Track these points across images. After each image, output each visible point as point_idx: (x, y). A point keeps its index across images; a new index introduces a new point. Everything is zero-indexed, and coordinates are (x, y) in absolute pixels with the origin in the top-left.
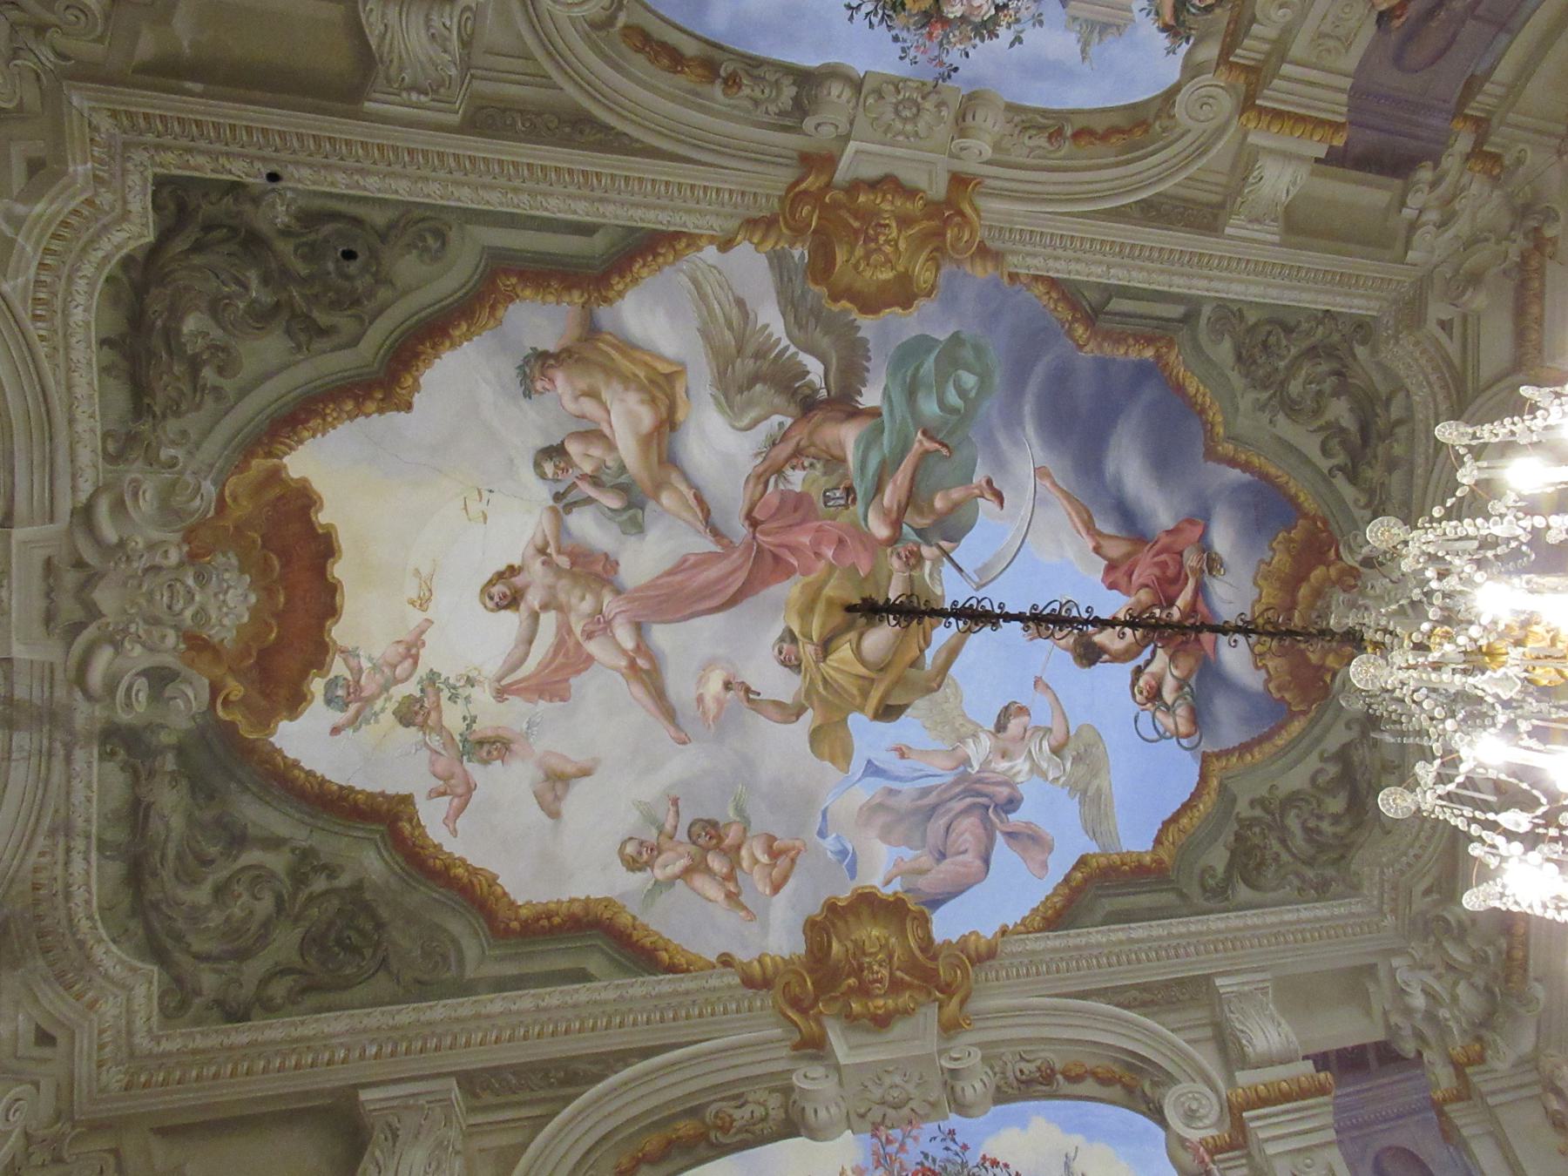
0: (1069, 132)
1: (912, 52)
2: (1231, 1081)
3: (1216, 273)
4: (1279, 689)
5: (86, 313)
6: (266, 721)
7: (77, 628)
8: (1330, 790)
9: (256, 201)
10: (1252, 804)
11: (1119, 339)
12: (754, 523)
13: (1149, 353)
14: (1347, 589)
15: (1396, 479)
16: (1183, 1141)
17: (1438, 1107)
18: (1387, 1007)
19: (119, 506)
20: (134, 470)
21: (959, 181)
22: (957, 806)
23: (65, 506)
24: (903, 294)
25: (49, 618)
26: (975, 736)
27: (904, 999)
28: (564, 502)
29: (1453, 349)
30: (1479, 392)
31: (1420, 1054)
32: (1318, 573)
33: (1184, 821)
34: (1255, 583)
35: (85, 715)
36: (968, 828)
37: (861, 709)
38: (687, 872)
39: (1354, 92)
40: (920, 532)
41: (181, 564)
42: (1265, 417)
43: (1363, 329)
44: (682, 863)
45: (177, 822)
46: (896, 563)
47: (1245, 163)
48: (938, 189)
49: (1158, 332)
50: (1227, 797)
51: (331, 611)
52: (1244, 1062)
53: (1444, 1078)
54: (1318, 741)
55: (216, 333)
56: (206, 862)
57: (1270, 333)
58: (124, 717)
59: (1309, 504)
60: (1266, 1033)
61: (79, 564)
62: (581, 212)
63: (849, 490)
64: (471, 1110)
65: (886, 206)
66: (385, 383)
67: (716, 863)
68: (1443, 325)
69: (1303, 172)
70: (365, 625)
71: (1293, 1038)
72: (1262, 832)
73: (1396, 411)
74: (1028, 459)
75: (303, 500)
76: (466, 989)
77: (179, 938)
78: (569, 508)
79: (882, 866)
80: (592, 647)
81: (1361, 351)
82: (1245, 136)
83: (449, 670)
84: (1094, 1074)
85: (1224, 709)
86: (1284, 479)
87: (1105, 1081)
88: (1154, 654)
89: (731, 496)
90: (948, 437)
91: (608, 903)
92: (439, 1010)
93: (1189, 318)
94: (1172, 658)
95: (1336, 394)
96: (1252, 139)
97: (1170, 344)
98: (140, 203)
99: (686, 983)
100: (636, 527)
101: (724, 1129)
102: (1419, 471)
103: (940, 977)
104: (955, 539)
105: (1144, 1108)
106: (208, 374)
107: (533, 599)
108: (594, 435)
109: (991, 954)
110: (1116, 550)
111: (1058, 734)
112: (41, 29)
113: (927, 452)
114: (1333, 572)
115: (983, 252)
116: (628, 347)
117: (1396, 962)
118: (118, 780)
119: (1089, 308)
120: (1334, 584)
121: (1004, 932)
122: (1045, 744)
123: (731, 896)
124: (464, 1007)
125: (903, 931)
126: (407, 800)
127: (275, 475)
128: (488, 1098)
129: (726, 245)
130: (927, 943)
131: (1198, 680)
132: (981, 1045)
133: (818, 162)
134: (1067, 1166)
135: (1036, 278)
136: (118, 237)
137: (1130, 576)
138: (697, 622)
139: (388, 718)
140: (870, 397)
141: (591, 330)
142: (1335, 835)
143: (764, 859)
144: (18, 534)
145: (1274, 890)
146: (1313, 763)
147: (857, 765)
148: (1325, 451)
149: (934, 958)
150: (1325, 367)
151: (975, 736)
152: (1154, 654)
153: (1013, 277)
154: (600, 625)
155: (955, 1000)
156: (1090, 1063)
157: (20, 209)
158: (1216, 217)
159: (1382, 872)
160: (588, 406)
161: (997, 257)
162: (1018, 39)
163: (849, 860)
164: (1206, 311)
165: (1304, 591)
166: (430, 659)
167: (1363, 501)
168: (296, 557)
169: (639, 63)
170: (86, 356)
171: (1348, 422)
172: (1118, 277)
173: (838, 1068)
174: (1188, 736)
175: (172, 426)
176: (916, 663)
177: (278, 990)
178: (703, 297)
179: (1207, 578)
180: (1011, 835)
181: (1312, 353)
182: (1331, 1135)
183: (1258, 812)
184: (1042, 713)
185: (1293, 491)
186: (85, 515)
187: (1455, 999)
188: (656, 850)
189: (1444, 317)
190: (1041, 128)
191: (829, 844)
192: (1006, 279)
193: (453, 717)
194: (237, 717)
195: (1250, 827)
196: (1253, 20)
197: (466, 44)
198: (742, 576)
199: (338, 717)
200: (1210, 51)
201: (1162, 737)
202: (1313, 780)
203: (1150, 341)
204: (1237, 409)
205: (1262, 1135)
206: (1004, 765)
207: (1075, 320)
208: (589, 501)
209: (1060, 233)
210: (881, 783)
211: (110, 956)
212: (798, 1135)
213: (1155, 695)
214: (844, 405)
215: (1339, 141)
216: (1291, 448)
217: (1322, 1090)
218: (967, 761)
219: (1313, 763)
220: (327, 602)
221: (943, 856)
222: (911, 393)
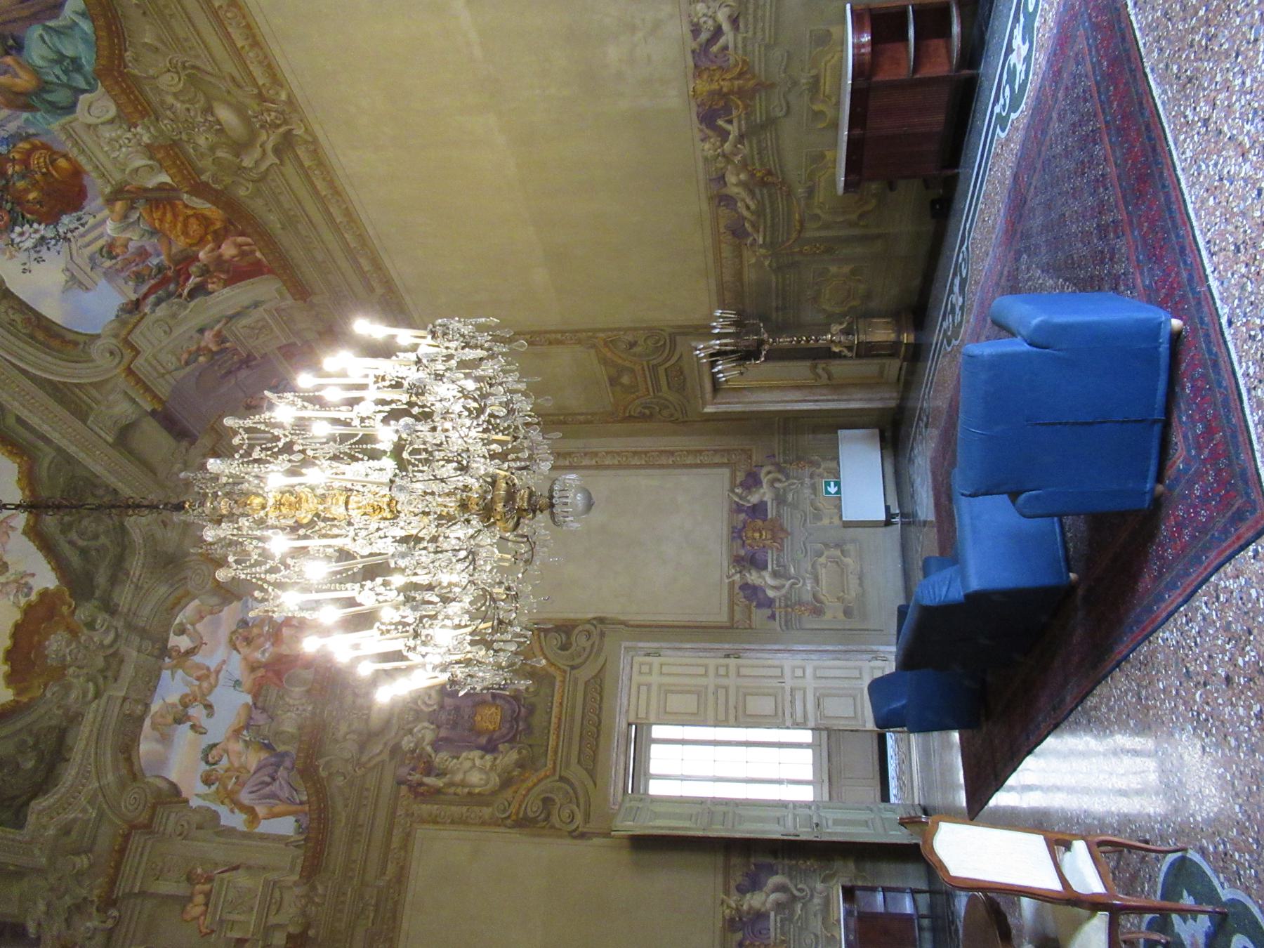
5: (69, 774)
7: (115, 654)
19: (85, 694)
23: (105, 698)
25: (122, 661)
41: (70, 666)
45: (102, 570)
51: (17, 627)
56: (97, 550)
58: (107, 616)
61: (105, 678)
64: (91, 409)
75: (11, 679)
76: (59, 450)
92: (72, 450)
98: (32, 819)
106: (31, 742)
112: (52, 889)
118: (115, 596)
124: (63, 443)
126: (25, 533)
127: (19, 693)
128: (84, 407)
139: (11, 571)
144: (122, 694)
170: (76, 756)
175: (54, 722)
177: (100, 492)
186: (98, 695)
194: (68, 598)
199: (31, 581)
212: (7, 290)
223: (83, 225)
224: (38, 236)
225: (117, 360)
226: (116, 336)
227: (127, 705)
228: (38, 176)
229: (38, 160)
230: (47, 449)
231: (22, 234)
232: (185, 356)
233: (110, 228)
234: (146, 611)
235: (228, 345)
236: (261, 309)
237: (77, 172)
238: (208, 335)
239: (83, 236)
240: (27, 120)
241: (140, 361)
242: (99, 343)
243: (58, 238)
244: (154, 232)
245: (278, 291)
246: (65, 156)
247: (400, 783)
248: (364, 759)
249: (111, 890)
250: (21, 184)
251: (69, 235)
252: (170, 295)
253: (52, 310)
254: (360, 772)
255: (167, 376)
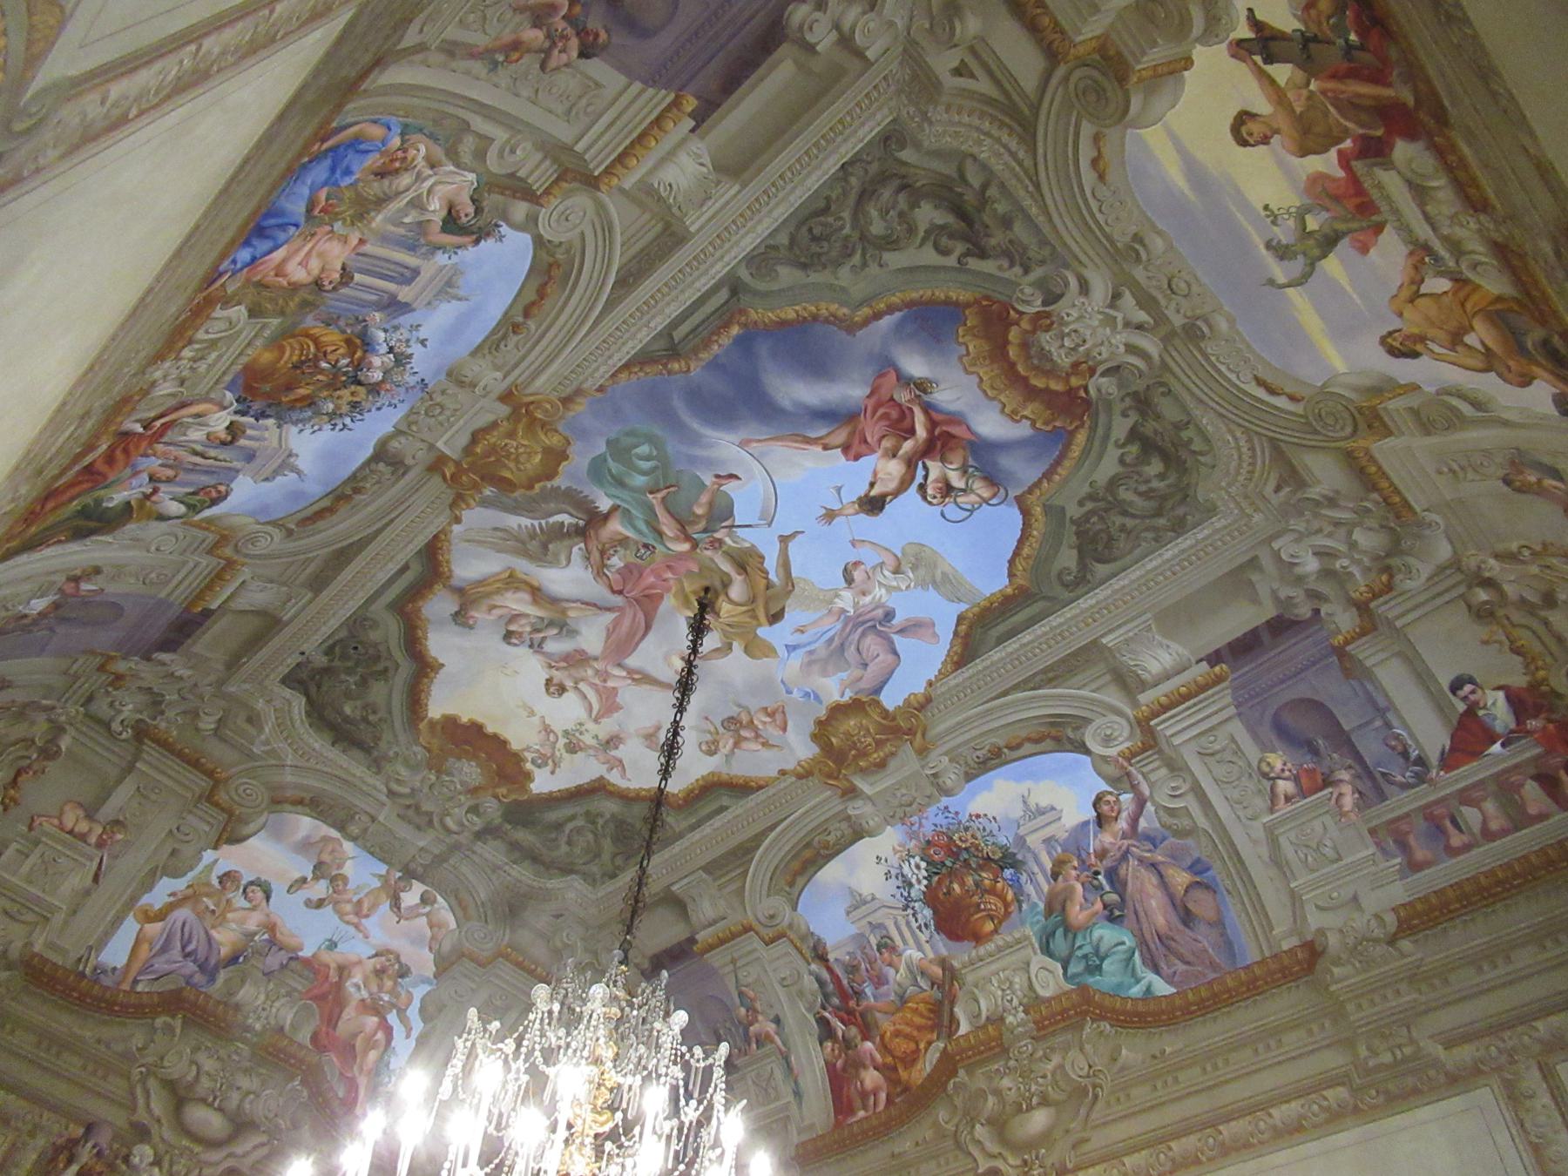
0: (520, 319)
1: (395, 401)
2: (1135, 704)
3: (718, 254)
4: (1046, 423)
5: (318, 742)
6: (524, 788)
7: (430, 823)
8: (1144, 458)
9: (309, 662)
10: (1081, 503)
11: (706, 344)
12: (620, 592)
13: (735, 330)
14: (1048, 329)
15: (1019, 229)
16: (1104, 758)
17: (1340, 652)
18: (1275, 586)
19: (398, 782)
20: (388, 768)
21: (506, 397)
22: (856, 636)
23: (384, 798)
24: (556, 457)
25: (419, 828)
26: (837, 596)
27: (888, 748)
28: (537, 647)
29: (984, 86)
30: (1036, 108)
31: (1317, 612)
32: (1014, 335)
33: (1026, 551)
34: (967, 372)
35: (464, 838)
36: (871, 644)
37: (760, 625)
38: (736, 745)
39: (651, 81)
40: (705, 531)
42: (873, 269)
43: (891, 139)
44: (731, 741)
46: (708, 553)
47: (647, 195)
48: (504, 410)
49: (725, 317)
50: (1055, 513)
51: (505, 743)
52: (1144, 686)
53: (1344, 620)
54: (1106, 437)
55: (359, 703)
57: (810, 230)
59: (964, 296)
60: (1158, 659)
61: (409, 807)
62: (393, 567)
63: (646, 546)
64: (715, 880)
65: (493, 440)
66: (424, 667)
67: (744, 733)
68: (958, 72)
69: (697, 145)
70: (520, 736)
71: (1181, 650)
72: (1101, 518)
73: (975, 180)
74: (726, 446)
75: (450, 723)
76: (681, 836)
77: (572, 863)
78: (540, 645)
79: (834, 688)
80: (610, 684)
81: (906, 155)
82: (622, 191)
83: (570, 726)
84: (1029, 739)
85: (1006, 462)
86: (929, 293)
87: (1037, 741)
88: (925, 468)
89: (596, 590)
90: (666, 481)
91: (713, 773)
93: (734, 292)
94: (943, 460)
95: (914, 205)
96: (627, 186)
97: (742, 312)
98: (287, 693)
99: (771, 791)
100: (573, 633)
101: (826, 848)
102: (1034, 211)
103: (905, 727)
104: (730, 514)
105: (1069, 747)
106: (371, 718)
107: (569, 684)
108: (515, 617)
109: (929, 700)
110: (841, 436)
111: (890, 562)
113: (663, 499)
114: (1025, 325)
115: (567, 401)
116: (481, 582)
117: (1276, 545)
118: (498, 843)
119: (668, 349)
120: (1034, 332)
121: (930, 684)
122: (886, 573)
123: (763, 744)
125: (867, 714)
126: (602, 778)
127: (432, 724)
129: (458, 520)
130: (885, 714)
131: (975, 460)
132: (945, 754)
133: (437, 465)
134: (1025, 802)
135: (614, 375)
136: (296, 711)
137: (866, 441)
138: (643, 645)
139: (565, 755)
140: (604, 504)
141: (460, 591)
142: (1169, 486)
143: (768, 719)
144: (381, 818)
145: (1130, 552)
146: (1113, 454)
147: (782, 652)
148: (945, 252)
149: (894, 719)
150: (886, 194)
151: (837, 596)
152: (925, 468)
153: (601, 389)
154: (605, 676)
155: (919, 735)
156: (1024, 734)
157: (263, 737)
158: (673, 234)
159: (1229, 493)
160: (497, 612)
161: (579, 392)
162: (423, 342)
163: (813, 696)
164: (744, 274)
165: (1013, 352)
166: (558, 728)
167: (1006, 264)
168: (470, 738)
169: (321, 524)
170: (334, 754)
171: (942, 217)
172: (659, 323)
173: (869, 798)
174: (994, 496)
175: (383, 745)
176: (769, 586)
178: (480, 542)
179: (926, 398)
180: (901, 631)
181: (865, 195)
182: (1232, 710)
183: (1089, 506)
184: (869, 557)
185: (942, 296)
186: (391, 794)
187: (1353, 545)
188: (715, 742)
189: (955, 64)
190: (504, 337)
191: (796, 694)
192: (599, 395)
193: (588, 739)
194: (514, 797)
195: (1088, 521)
196: (512, 175)
197: (272, 582)
198: (641, 616)
200: (520, 209)
201: (971, 512)
202: (1122, 461)
203: (727, 326)
204: (843, 289)
205: (1168, 733)
206: (868, 599)
207: (665, 365)
208: (544, 638)
209: (594, 345)
210: (801, 652)
211: (553, 883)
213: (947, 489)
214: (596, 519)
215: (690, 104)
216: (912, 270)
217: (1219, 680)
218: (843, 611)
219: (1113, 454)
220: (499, 743)
221: (866, 665)
222: (620, 483)
223: (919, 928)
224: (914, 881)
225: (763, 919)
226: (790, 926)
227: (365, 818)
228: (976, 899)
229: (993, 903)
230: (684, 825)
231: (918, 867)
232: (751, 994)
233: (913, 954)
234: (465, 869)
235: (754, 1046)
236: (791, 1098)
237: (978, 938)
238: (771, 1027)
239: (908, 923)
240: (1035, 905)
241: (757, 943)
242: (788, 909)
243: (908, 899)
244: (903, 999)
245: (812, 1126)
246: (996, 931)
247: (90, 1128)
248: (152, 1084)
249: (157, 741)
250: (970, 881)
251: (910, 911)
252: (826, 996)
253: (831, 872)
254: (136, 1072)
255: (731, 967)
